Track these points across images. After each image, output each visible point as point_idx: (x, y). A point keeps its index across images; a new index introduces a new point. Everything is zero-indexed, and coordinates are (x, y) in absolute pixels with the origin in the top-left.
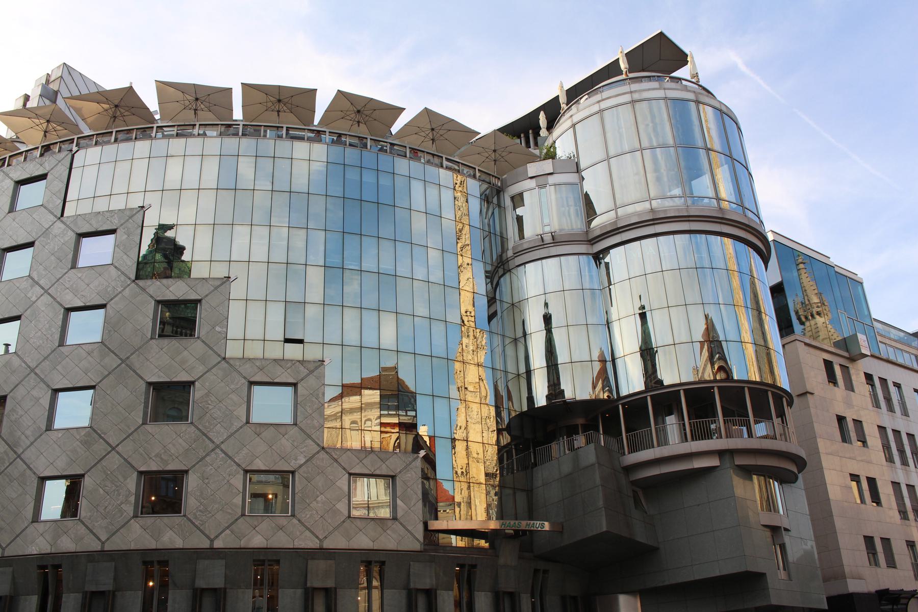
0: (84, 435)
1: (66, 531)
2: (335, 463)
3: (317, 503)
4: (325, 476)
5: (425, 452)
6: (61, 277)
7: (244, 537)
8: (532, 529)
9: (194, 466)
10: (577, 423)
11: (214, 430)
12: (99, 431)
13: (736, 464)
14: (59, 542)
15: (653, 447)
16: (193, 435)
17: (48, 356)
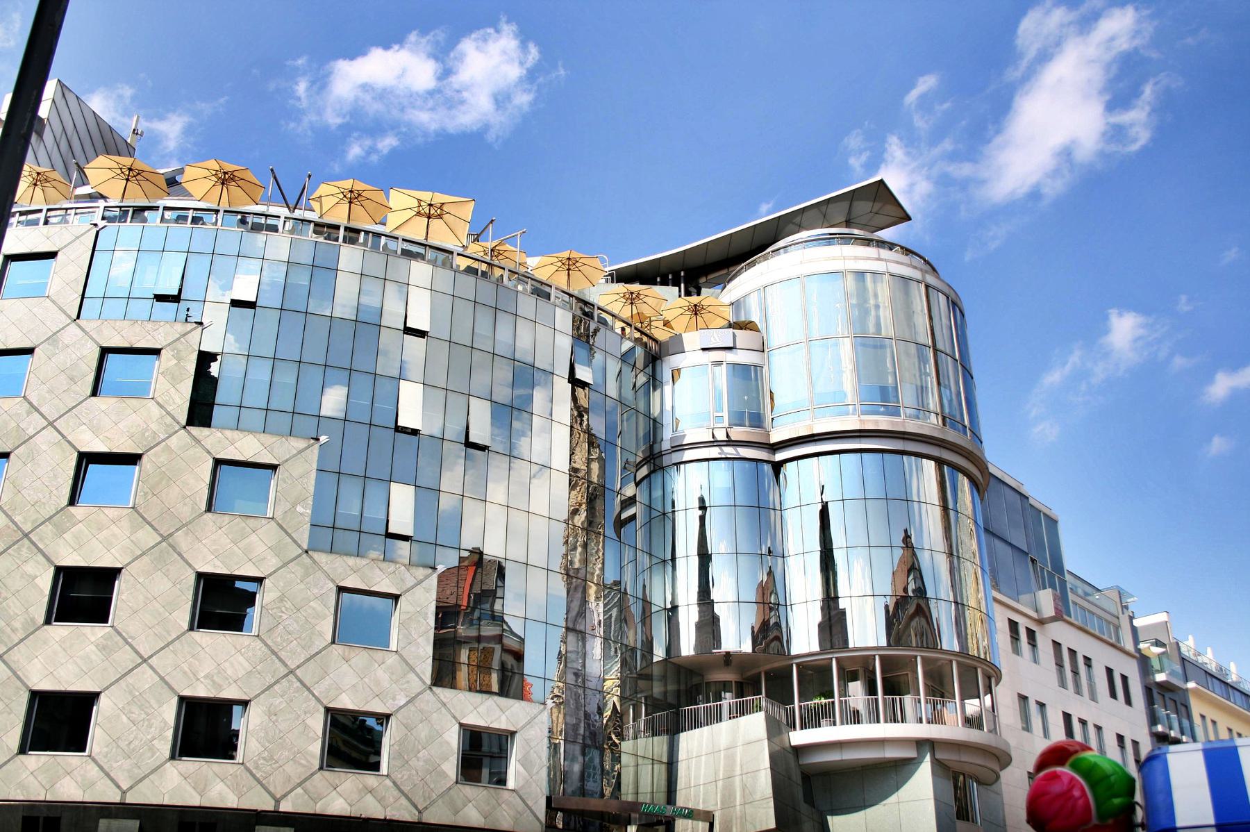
2: (443, 709)
3: (418, 760)
4: (430, 725)
7: (321, 799)
9: (258, 695)
12: (124, 634)
14: (58, 785)
16: (259, 653)
17: (51, 518)
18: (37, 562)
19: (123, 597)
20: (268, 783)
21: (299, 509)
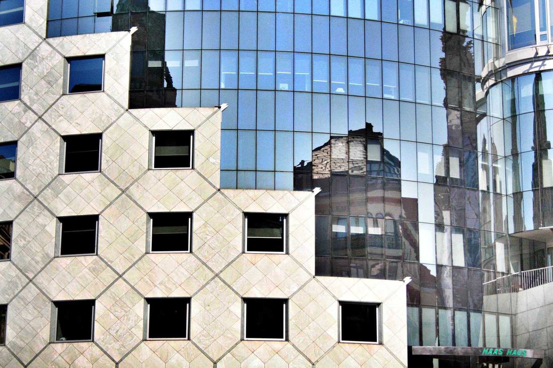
0: (91, 263)
1: (82, 352)
3: (309, 329)
4: (316, 304)
5: (410, 279)
6: (53, 104)
9: (196, 293)
12: (105, 260)
14: (76, 362)
16: (194, 264)
17: (49, 184)
18: (45, 215)
19: (101, 235)
20: (208, 351)
21: (212, 160)
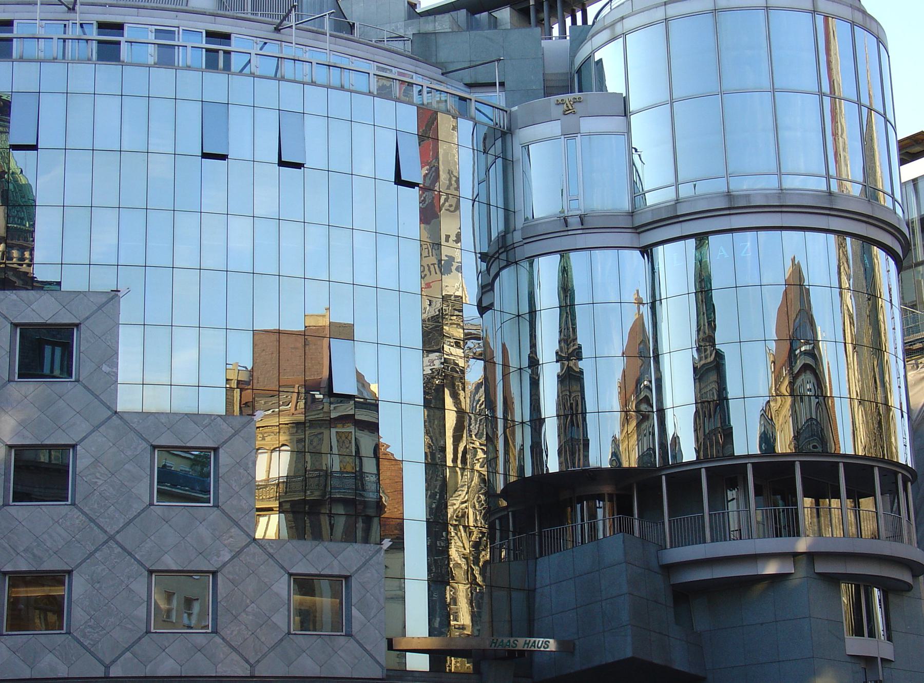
3: (247, 615)
4: (257, 578)
8: (533, 648)
10: (603, 492)
11: (106, 514)
13: (816, 571)
15: (705, 542)
16: (77, 521)
